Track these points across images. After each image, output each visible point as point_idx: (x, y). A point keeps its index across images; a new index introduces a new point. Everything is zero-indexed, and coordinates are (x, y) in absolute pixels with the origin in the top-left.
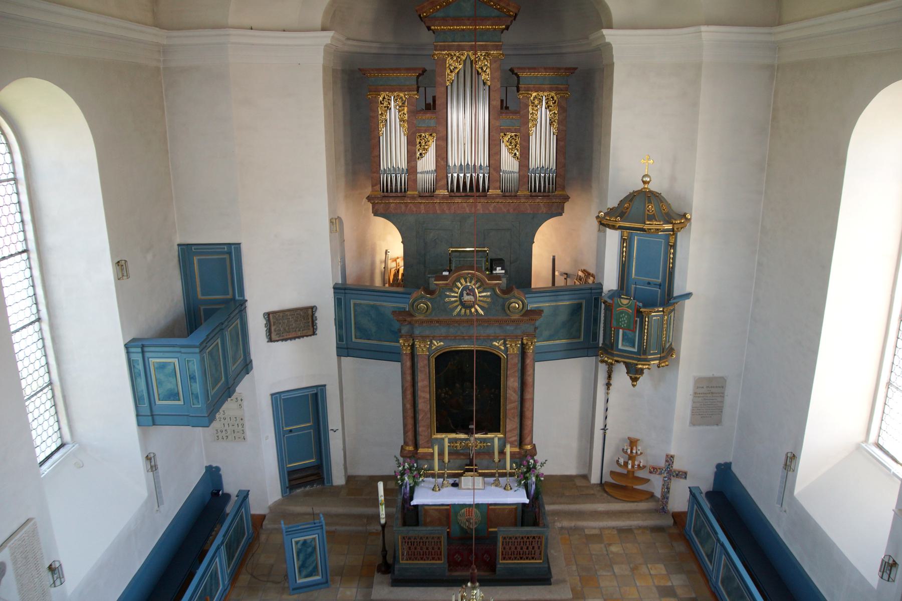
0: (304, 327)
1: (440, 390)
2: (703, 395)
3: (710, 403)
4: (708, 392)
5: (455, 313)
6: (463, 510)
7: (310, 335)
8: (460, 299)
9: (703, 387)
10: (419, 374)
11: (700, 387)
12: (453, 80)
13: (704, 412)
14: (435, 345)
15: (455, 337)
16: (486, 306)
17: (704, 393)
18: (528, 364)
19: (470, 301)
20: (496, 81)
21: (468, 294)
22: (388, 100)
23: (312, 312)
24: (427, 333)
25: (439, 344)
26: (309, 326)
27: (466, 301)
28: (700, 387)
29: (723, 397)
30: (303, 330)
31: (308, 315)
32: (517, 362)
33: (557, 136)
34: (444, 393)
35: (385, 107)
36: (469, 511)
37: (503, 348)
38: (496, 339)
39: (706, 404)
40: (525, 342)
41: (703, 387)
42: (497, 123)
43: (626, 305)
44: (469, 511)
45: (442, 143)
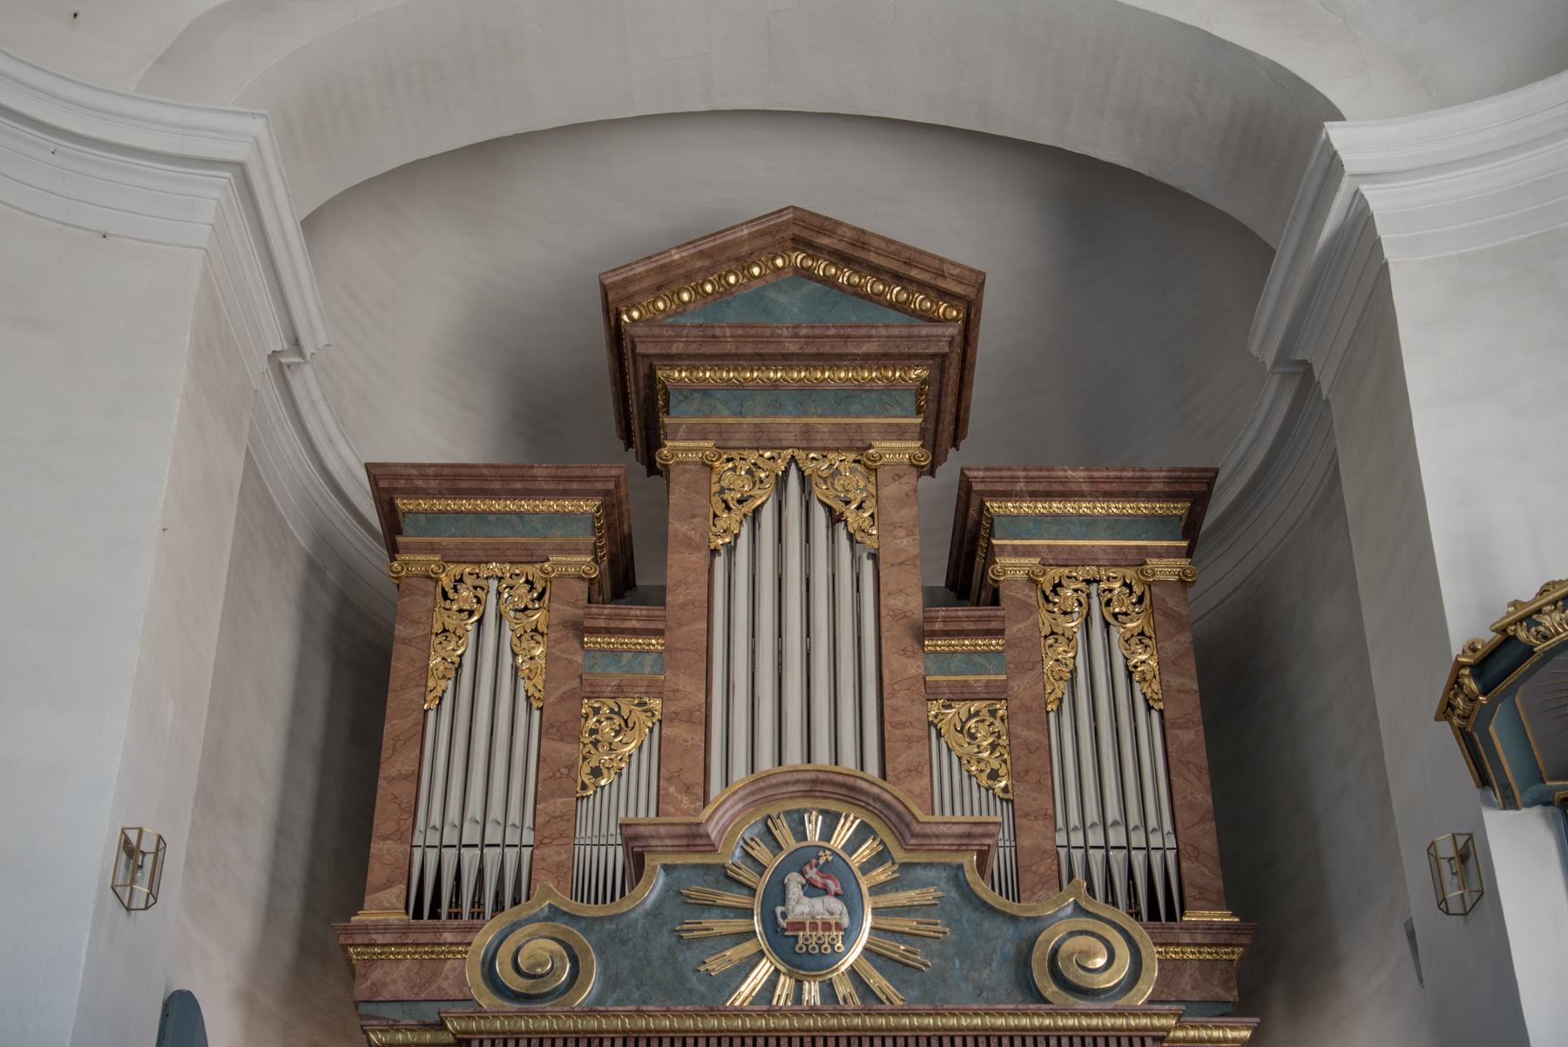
12: (737, 536)
19: (827, 926)
20: (902, 533)
21: (811, 889)
27: (800, 926)
33: (1161, 712)
35: (461, 611)
42: (914, 667)
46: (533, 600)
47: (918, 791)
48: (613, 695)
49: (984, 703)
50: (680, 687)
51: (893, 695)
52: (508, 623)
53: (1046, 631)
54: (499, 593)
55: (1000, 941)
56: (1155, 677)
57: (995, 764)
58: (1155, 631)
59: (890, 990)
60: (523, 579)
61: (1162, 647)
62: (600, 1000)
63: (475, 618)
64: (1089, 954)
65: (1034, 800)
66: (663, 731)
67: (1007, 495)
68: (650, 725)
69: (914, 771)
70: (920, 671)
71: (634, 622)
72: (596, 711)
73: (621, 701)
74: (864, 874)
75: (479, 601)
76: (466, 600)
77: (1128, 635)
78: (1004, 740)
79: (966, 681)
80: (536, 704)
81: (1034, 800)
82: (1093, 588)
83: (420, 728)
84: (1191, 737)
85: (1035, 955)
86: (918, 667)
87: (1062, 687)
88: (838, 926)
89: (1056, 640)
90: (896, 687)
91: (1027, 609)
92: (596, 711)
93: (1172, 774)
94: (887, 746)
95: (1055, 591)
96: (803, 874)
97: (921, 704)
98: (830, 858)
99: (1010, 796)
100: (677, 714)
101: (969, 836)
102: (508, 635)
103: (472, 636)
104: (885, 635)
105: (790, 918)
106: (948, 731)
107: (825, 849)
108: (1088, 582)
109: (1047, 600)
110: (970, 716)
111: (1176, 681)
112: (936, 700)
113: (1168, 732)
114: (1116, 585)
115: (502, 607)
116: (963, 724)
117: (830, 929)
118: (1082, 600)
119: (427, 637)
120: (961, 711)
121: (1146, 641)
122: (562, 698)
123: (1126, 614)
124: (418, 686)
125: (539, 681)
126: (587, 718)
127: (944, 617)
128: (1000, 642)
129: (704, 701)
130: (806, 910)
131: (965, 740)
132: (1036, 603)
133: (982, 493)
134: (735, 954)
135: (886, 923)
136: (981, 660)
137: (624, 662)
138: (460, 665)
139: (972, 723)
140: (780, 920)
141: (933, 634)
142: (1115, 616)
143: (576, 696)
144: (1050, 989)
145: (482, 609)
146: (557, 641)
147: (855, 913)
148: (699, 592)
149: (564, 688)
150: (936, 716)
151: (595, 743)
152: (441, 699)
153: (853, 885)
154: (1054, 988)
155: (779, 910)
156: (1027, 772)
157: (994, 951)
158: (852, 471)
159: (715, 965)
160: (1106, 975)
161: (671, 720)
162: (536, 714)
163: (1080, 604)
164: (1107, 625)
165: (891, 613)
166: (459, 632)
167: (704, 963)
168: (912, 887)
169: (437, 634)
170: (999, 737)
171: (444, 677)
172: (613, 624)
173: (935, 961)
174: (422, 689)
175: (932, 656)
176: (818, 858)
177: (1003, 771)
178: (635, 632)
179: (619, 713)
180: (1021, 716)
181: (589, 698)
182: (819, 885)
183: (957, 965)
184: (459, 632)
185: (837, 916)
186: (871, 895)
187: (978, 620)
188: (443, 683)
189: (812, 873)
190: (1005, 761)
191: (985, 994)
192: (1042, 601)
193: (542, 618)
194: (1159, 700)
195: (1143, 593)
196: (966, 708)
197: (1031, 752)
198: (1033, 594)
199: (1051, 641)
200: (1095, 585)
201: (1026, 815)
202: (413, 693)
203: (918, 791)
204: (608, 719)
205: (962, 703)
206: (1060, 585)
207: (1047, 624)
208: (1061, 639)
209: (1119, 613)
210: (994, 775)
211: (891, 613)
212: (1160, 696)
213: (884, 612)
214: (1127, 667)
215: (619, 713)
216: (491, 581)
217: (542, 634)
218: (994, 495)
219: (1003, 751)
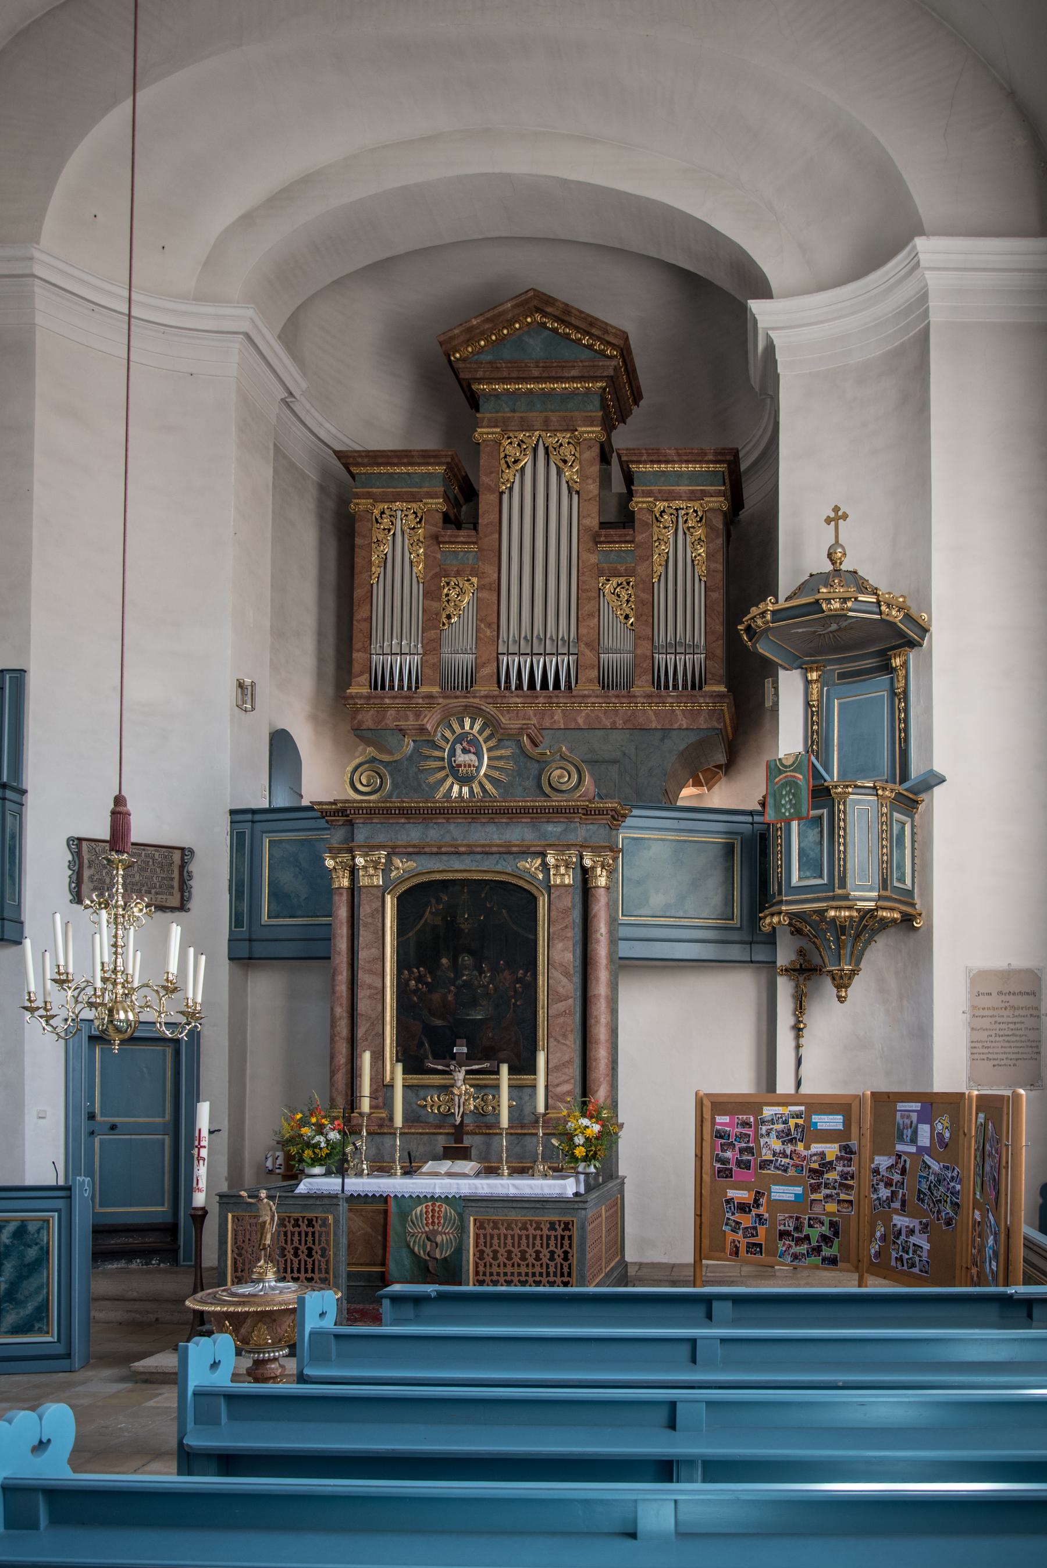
0: (161, 887)
2: (991, 1013)
3: (1010, 1033)
4: (1004, 1005)
5: (439, 796)
7: (173, 909)
8: (450, 762)
9: (990, 994)
10: (361, 932)
11: (983, 994)
13: (997, 1053)
14: (398, 868)
15: (440, 847)
16: (503, 778)
17: (994, 1008)
18: (595, 916)
19: (470, 766)
21: (465, 751)
23: (182, 859)
25: (406, 865)
26: (172, 887)
27: (460, 766)
28: (983, 994)
29: (1038, 1017)
30: (157, 893)
31: (171, 864)
32: (570, 905)
37: (541, 876)
38: (526, 852)
39: (1001, 1033)
41: (990, 994)
43: (790, 766)
51: (583, 574)
53: (655, 538)
59: (494, 791)
67: (639, 462)
83: (369, 594)
84: (717, 596)
88: (474, 766)
91: (648, 526)
92: (448, 584)
95: (661, 515)
101: (522, 729)
102: (407, 541)
103: (390, 542)
108: (677, 510)
109: (658, 521)
111: (713, 566)
119: (370, 544)
121: (702, 543)
122: (432, 578)
123: (693, 527)
131: (614, 597)
133: (627, 462)
136: (624, 555)
138: (386, 558)
142: (689, 528)
143: (437, 576)
144: (547, 790)
146: (429, 547)
149: (433, 572)
151: (448, 601)
155: (453, 759)
158: (569, 443)
159: (432, 780)
161: (482, 589)
162: (421, 585)
164: (685, 533)
168: (503, 748)
172: (452, 540)
179: (458, 585)
180: (641, 586)
187: (620, 536)
188: (378, 569)
189: (465, 744)
192: (655, 521)
202: (365, 575)
204: (454, 588)
215: (458, 585)
218: (633, 462)
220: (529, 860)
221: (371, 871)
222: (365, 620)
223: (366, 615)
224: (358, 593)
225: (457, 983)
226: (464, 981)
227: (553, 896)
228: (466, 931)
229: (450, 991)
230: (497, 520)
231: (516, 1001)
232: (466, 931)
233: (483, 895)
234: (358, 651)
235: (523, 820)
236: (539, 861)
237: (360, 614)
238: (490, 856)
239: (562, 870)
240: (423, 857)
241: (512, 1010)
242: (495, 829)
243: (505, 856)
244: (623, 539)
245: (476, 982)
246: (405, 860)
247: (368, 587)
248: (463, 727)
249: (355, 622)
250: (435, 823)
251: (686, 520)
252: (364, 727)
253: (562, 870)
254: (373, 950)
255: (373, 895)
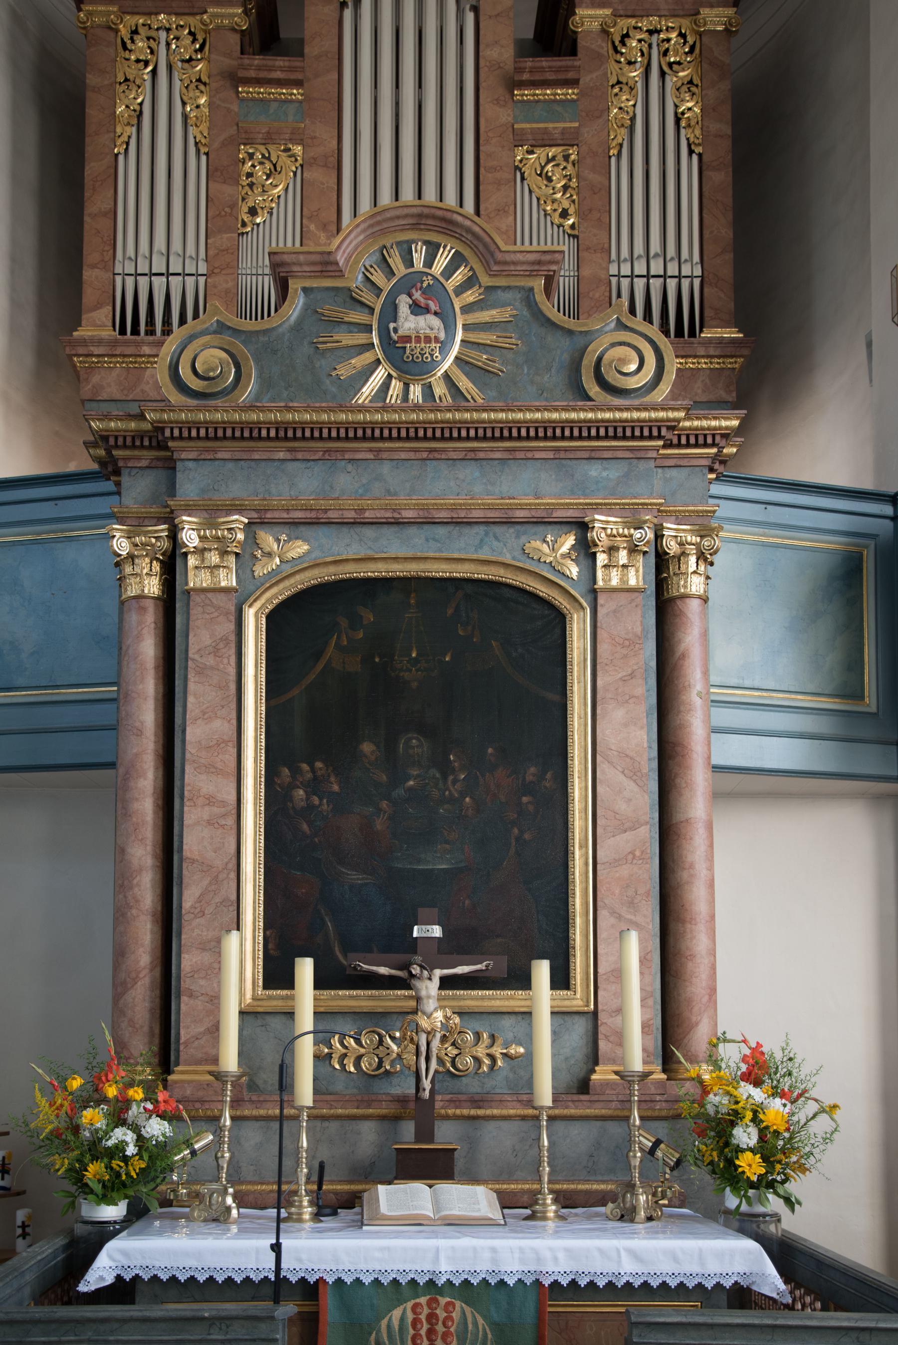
1: (286, 771)
6: (397, 1313)
14: (269, 555)
19: (428, 339)
21: (417, 309)
22: (148, 38)
24: (236, 490)
27: (407, 339)
34: (305, 786)
36: (432, 1317)
40: (672, 547)
42: (504, 115)
44: (432, 1317)
45: (320, 176)
46: (196, 51)
47: (504, 228)
48: (264, 142)
49: (560, 149)
50: (317, 135)
52: (176, 73)
53: (613, 80)
54: (168, 44)
55: (559, 352)
56: (698, 123)
57: (566, 204)
58: (701, 80)
60: (187, 31)
61: (706, 95)
62: (258, 398)
63: (150, 68)
64: (624, 361)
65: (595, 235)
66: (305, 175)
68: (294, 169)
69: (501, 211)
70: (510, 119)
71: (279, 73)
72: (251, 156)
73: (271, 148)
74: (457, 296)
75: (152, 52)
76: (141, 50)
77: (679, 84)
78: (574, 183)
79: (546, 128)
80: (203, 150)
81: (595, 235)
82: (654, 38)
83: (113, 171)
84: (721, 177)
85: (585, 362)
86: (509, 115)
87: (624, 132)
88: (437, 340)
89: (621, 89)
90: (490, 134)
91: (599, 59)
92: (251, 156)
93: (705, 211)
94: (481, 188)
95: (623, 43)
96: (410, 295)
97: (510, 150)
98: (431, 282)
99: (576, 232)
100: (315, 159)
101: (539, 263)
102: (177, 84)
103: (148, 85)
104: (483, 85)
105: (400, 332)
106: (530, 175)
107: (427, 274)
108: (651, 32)
110: (549, 161)
111: (714, 127)
112: (522, 146)
113: (705, 173)
114: (673, 35)
115: (171, 58)
116: (543, 168)
117: (430, 342)
118: (644, 50)
120: (542, 156)
121: (694, 89)
123: (679, 63)
124: (108, 132)
125: (204, 127)
126: (243, 163)
127: (531, 68)
128: (576, 91)
129: (336, 147)
130: (413, 326)
131: (543, 182)
132: (606, 54)
134: (360, 361)
135: (473, 337)
136: (559, 108)
137: (271, 111)
138: (141, 113)
139: (549, 167)
140: (392, 334)
141: (521, 85)
142: (670, 65)
144: (593, 389)
145: (155, 59)
147: (450, 328)
148: (330, 44)
150: (521, 161)
151: (251, 185)
152: (128, 144)
153: (449, 305)
154: (597, 389)
156: (590, 210)
157: (554, 359)
159: (344, 371)
160: (636, 378)
161: (311, 165)
162: (204, 158)
163: (643, 55)
164: (663, 74)
165: (488, 64)
166: (138, 82)
167: (335, 369)
168: (493, 306)
169: (120, 83)
170: (570, 180)
171: (128, 124)
172: (263, 75)
173: (509, 367)
174: (112, 135)
175: (519, 105)
176: (422, 282)
177: (571, 211)
178: (280, 83)
179: (269, 159)
181: (245, 144)
182: (422, 305)
183: (526, 371)
184: (138, 82)
185: (435, 331)
186: (462, 314)
187: (558, 70)
188: (128, 129)
189: (417, 295)
190: (573, 201)
191: (545, 394)
192: (611, 51)
193: (204, 69)
194: (699, 145)
195: (695, 43)
196: (544, 153)
197: (595, 193)
198: (604, 45)
199: (616, 90)
200: (656, 35)
201: (588, 249)
203: (504, 228)
204: (261, 163)
205: (542, 149)
206: (627, 35)
207: (614, 73)
208: (625, 88)
209: (674, 63)
210: (564, 214)
211: (488, 64)
212: (700, 140)
213: (482, 63)
214: (676, 113)
215: (269, 159)
216: (161, 32)
217: (205, 84)
219: (573, 192)
220: (549, 538)
221: (214, 558)
222: (105, 214)
223: (107, 206)
224: (92, 169)
225: (395, 794)
226: (410, 789)
227: (601, 612)
228: (415, 685)
229: (379, 810)
230: (336, 49)
231: (522, 832)
232: (415, 685)
233: (450, 612)
234: (93, 266)
235: (538, 455)
236: (569, 541)
237: (95, 204)
238: (466, 530)
239: (623, 557)
240: (322, 531)
241: (512, 851)
242: (477, 474)
243: (498, 529)
244: (561, 76)
245: (435, 793)
246: (284, 537)
247: (110, 159)
248: (410, 263)
249: (86, 218)
250: (350, 460)
251: (667, 50)
252: (104, 396)
253: (623, 557)
254: (217, 724)
255: (218, 608)
